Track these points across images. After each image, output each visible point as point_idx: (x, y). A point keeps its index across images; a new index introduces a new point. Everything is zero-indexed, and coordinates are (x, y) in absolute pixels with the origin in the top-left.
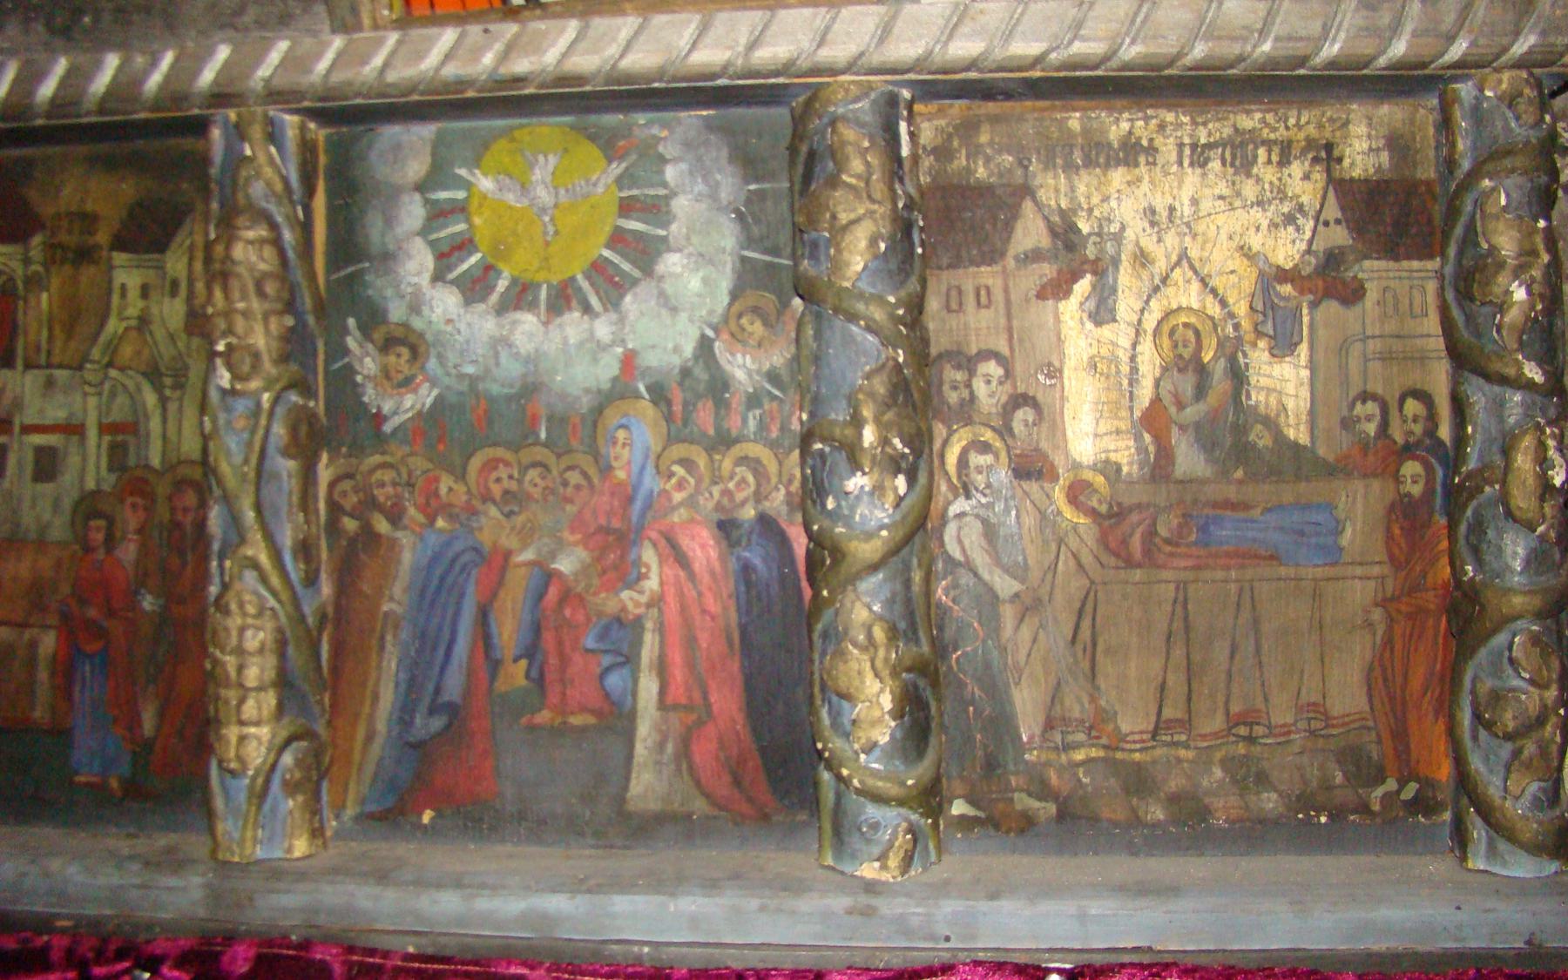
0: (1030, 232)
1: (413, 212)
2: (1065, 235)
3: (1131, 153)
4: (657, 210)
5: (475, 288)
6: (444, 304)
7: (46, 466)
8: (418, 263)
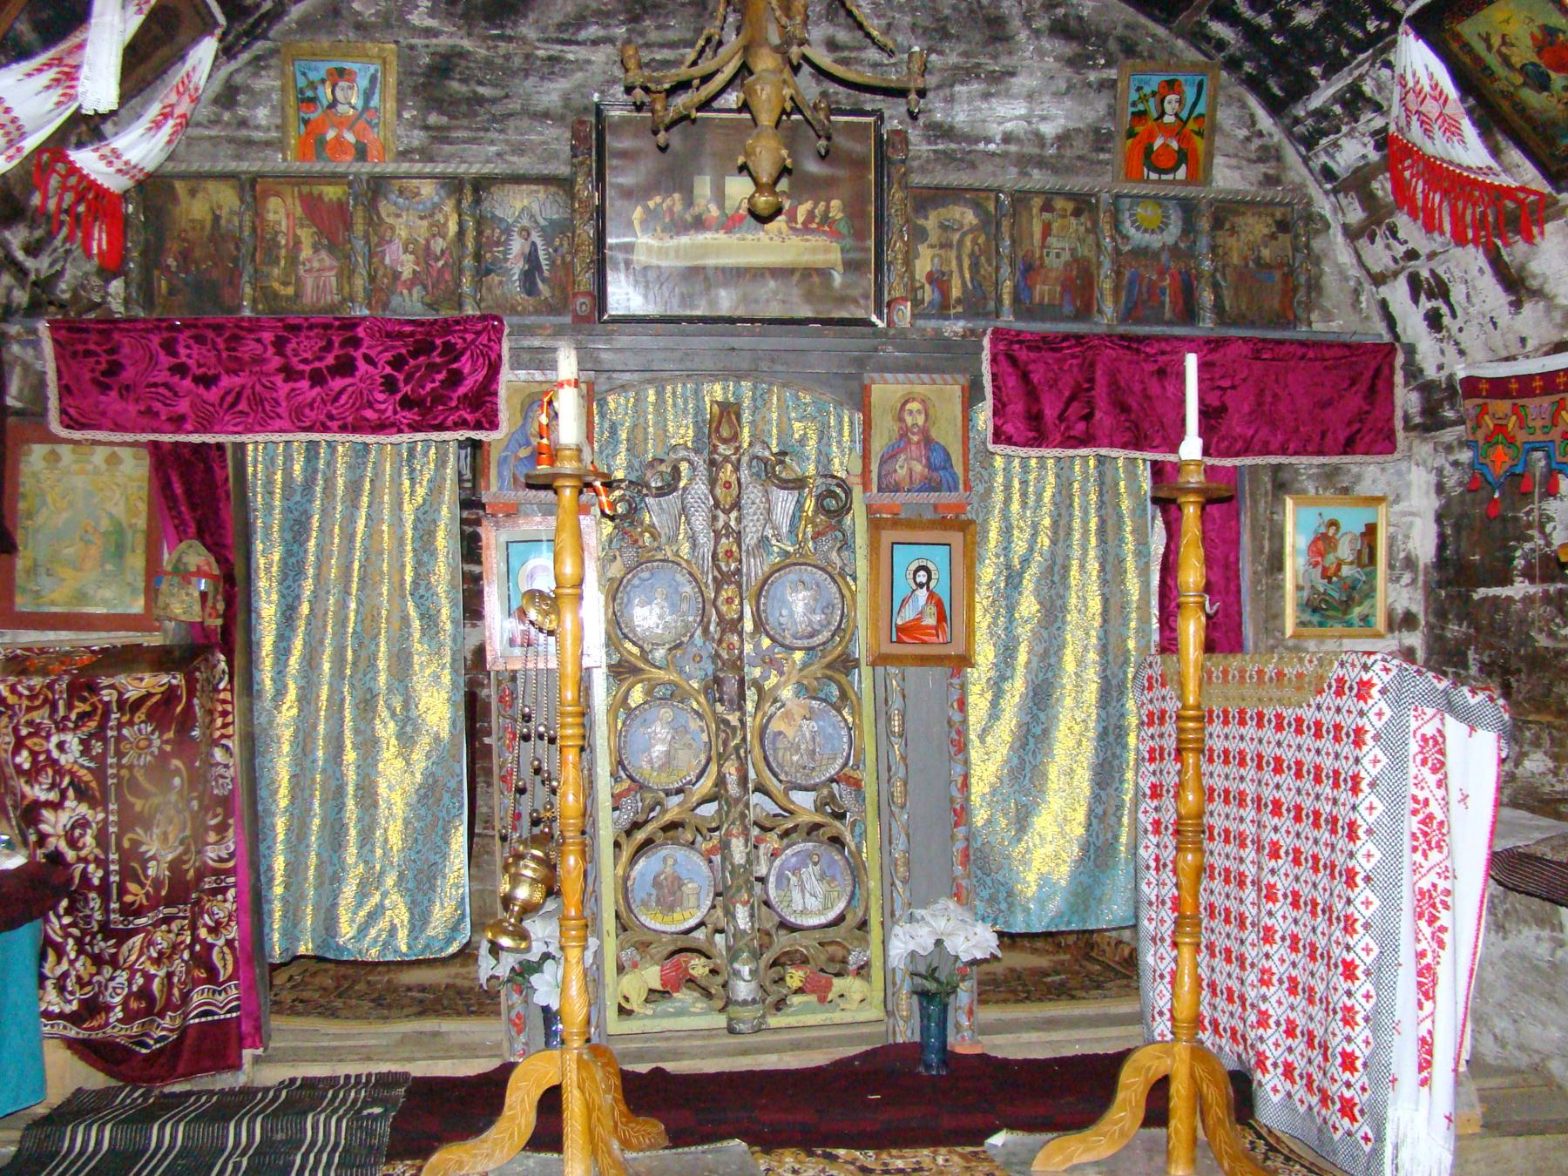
0: (1227, 226)
1: (1127, 214)
2: (1233, 227)
3: (1244, 213)
4: (1168, 217)
5: (1138, 228)
6: (1132, 231)
7: (1058, 255)
8: (1128, 223)
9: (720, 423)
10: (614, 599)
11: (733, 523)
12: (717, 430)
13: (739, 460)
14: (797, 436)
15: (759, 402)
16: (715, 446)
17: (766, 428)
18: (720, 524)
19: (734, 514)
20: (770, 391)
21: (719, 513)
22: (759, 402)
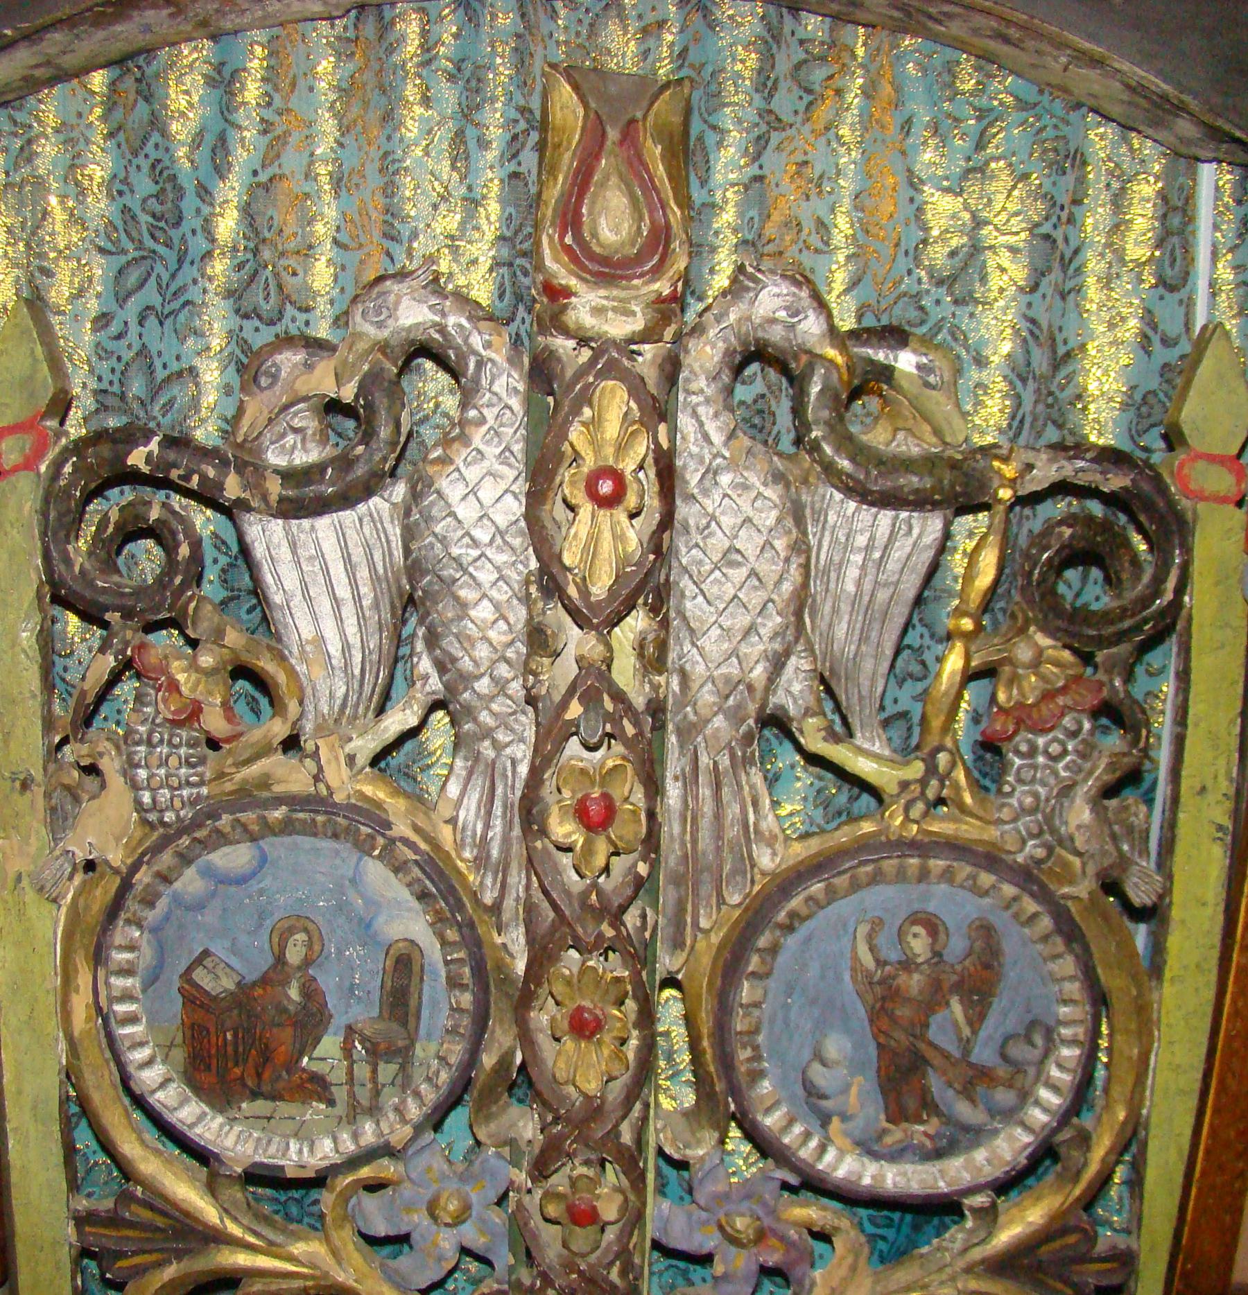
9: (582, 180)
10: (98, 957)
11: (625, 672)
12: (570, 219)
13: (672, 369)
14: (937, 255)
15: (786, 102)
16: (556, 293)
17: (806, 212)
18: (564, 671)
19: (638, 622)
20: (836, 50)
21: (556, 615)
22: (786, 102)
